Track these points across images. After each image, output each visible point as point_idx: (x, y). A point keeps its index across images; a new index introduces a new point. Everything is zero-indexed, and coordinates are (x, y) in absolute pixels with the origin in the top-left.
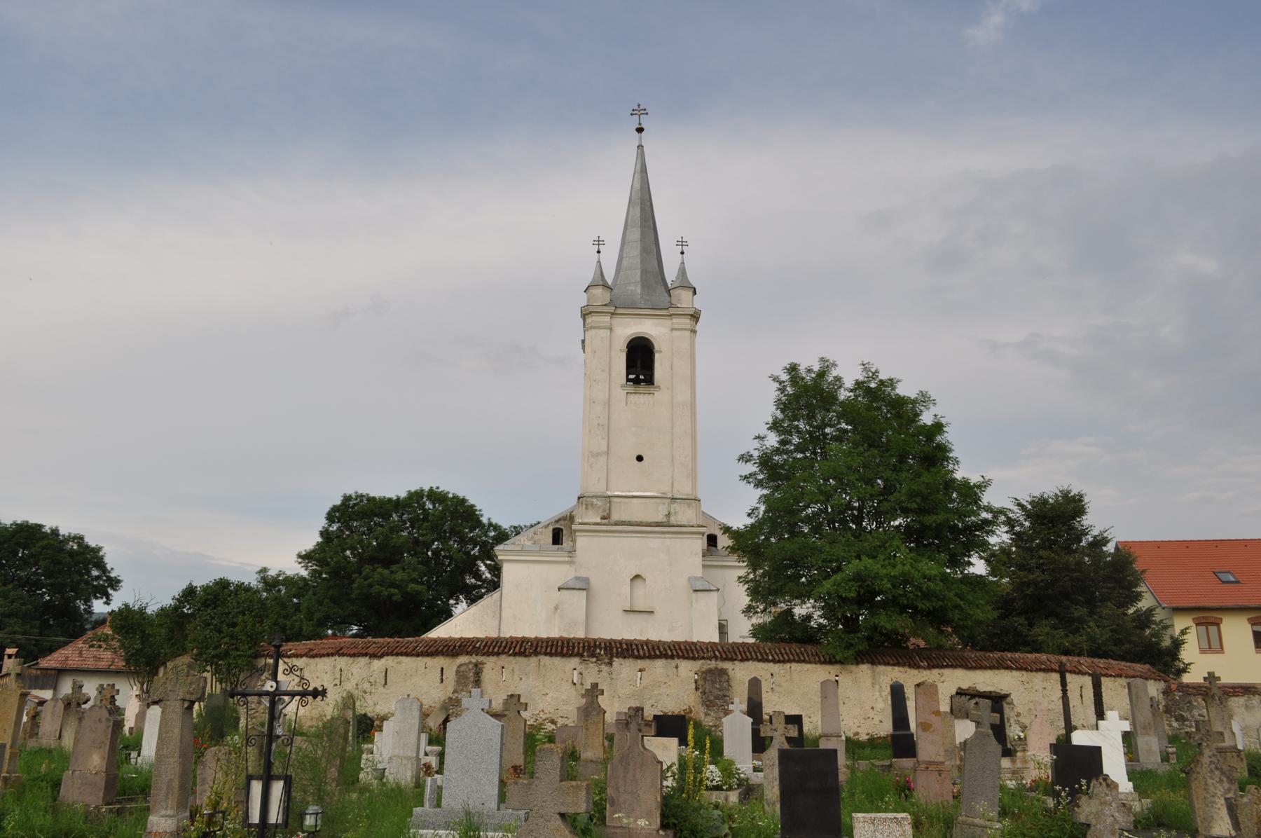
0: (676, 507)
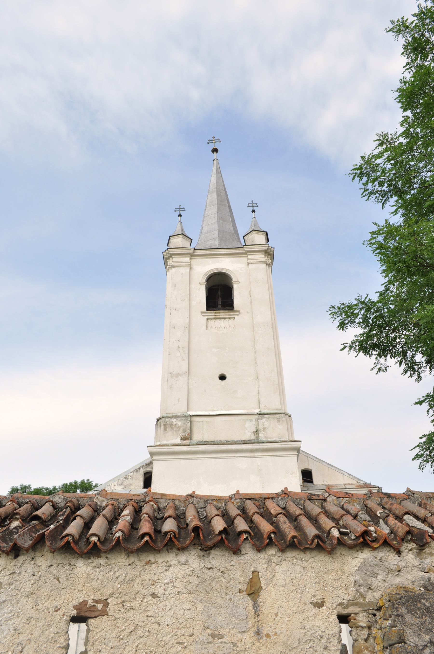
0: (264, 422)
